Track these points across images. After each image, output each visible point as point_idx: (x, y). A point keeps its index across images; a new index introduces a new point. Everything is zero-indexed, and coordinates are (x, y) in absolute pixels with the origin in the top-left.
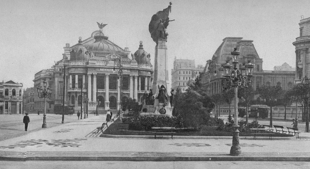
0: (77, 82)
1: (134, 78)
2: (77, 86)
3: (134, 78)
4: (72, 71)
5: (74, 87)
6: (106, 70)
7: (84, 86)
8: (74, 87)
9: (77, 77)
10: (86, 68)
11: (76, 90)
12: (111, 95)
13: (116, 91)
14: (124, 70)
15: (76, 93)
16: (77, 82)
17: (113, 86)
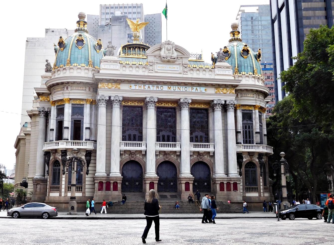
0: (67, 122)
1: (225, 108)
2: (67, 134)
3: (225, 108)
4: (57, 96)
5: (60, 137)
6: (149, 87)
7: (86, 134)
8: (60, 137)
9: (68, 110)
10: (94, 86)
11: (62, 145)
12: (162, 158)
13: (175, 146)
14: (198, 88)
15: (64, 152)
16: (67, 122)
17: (167, 132)
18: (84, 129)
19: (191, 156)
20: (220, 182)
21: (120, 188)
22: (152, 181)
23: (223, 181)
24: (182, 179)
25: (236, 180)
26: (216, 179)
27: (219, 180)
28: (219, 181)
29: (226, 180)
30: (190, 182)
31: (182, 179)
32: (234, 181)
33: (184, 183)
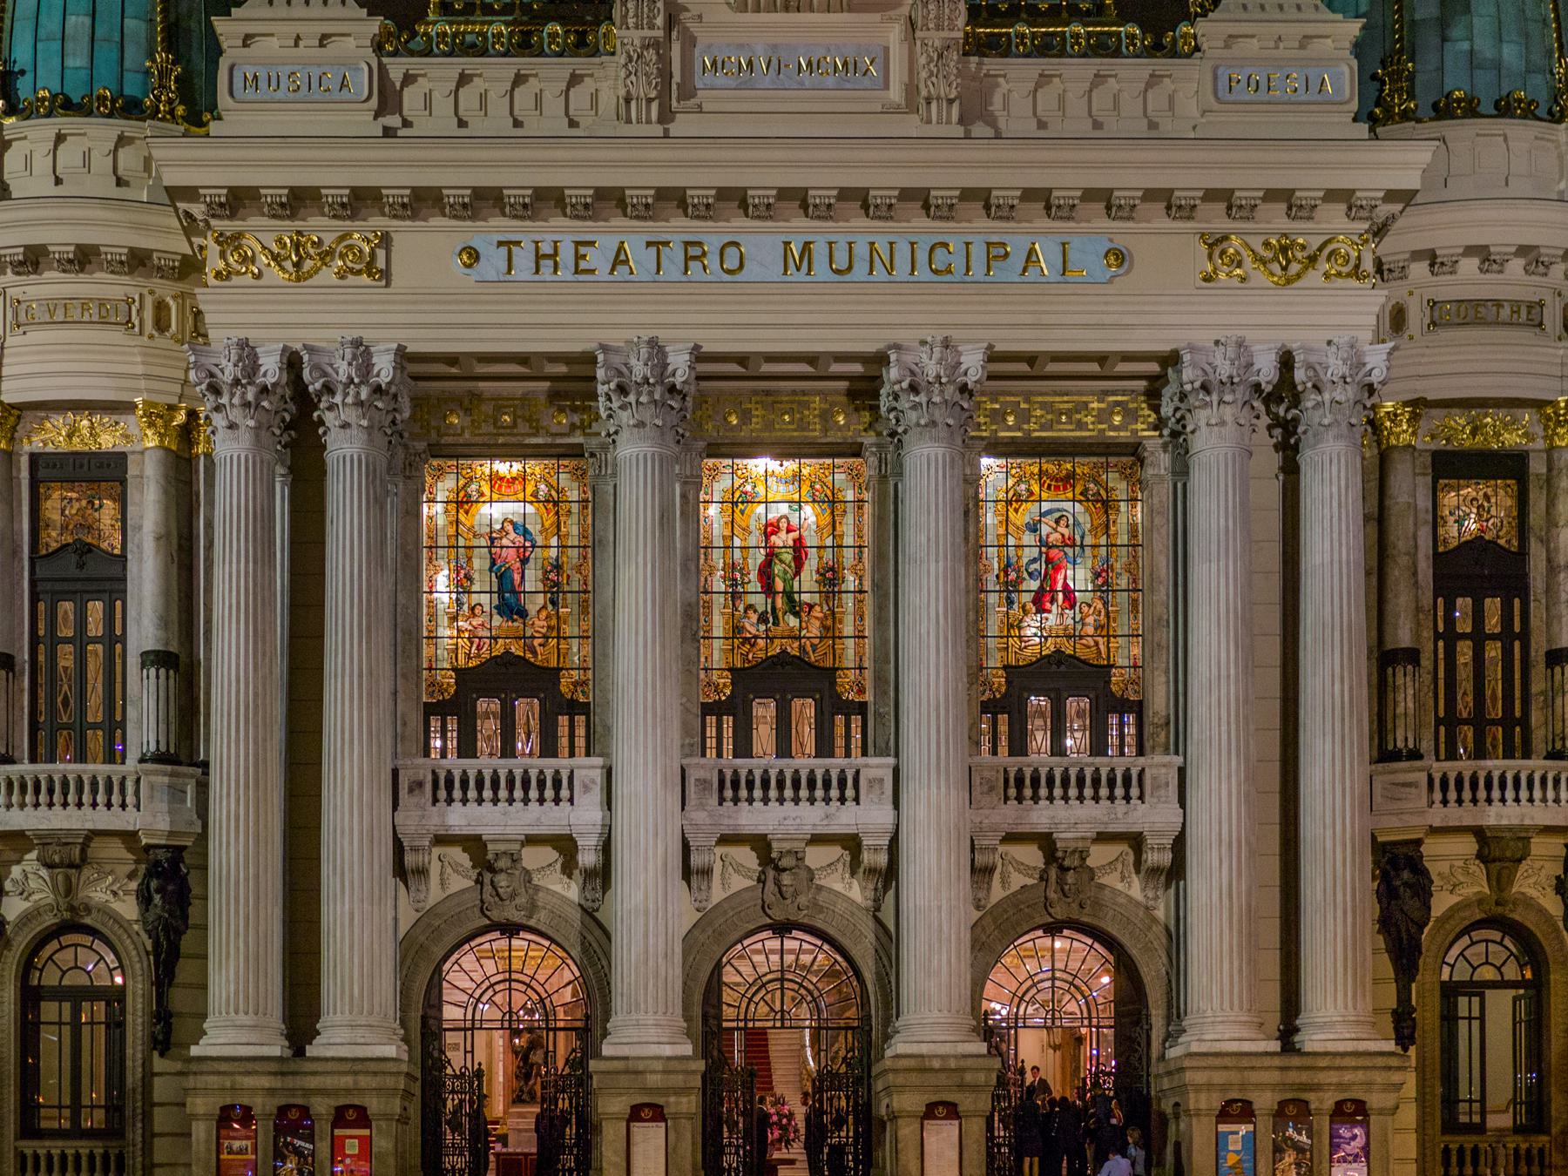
18: (133, 661)
19: (981, 873)
20: (1216, 1102)
21: (391, 1161)
22: (647, 1100)
23: (1243, 1086)
24: (900, 1079)
25: (1360, 1076)
26: (1189, 1076)
27: (1219, 1078)
28: (1209, 1087)
29: (1275, 1076)
30: (965, 1102)
31: (900, 1079)
32: (1340, 1086)
33: (911, 1115)
